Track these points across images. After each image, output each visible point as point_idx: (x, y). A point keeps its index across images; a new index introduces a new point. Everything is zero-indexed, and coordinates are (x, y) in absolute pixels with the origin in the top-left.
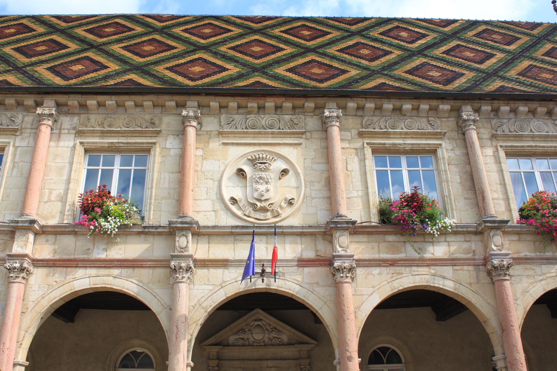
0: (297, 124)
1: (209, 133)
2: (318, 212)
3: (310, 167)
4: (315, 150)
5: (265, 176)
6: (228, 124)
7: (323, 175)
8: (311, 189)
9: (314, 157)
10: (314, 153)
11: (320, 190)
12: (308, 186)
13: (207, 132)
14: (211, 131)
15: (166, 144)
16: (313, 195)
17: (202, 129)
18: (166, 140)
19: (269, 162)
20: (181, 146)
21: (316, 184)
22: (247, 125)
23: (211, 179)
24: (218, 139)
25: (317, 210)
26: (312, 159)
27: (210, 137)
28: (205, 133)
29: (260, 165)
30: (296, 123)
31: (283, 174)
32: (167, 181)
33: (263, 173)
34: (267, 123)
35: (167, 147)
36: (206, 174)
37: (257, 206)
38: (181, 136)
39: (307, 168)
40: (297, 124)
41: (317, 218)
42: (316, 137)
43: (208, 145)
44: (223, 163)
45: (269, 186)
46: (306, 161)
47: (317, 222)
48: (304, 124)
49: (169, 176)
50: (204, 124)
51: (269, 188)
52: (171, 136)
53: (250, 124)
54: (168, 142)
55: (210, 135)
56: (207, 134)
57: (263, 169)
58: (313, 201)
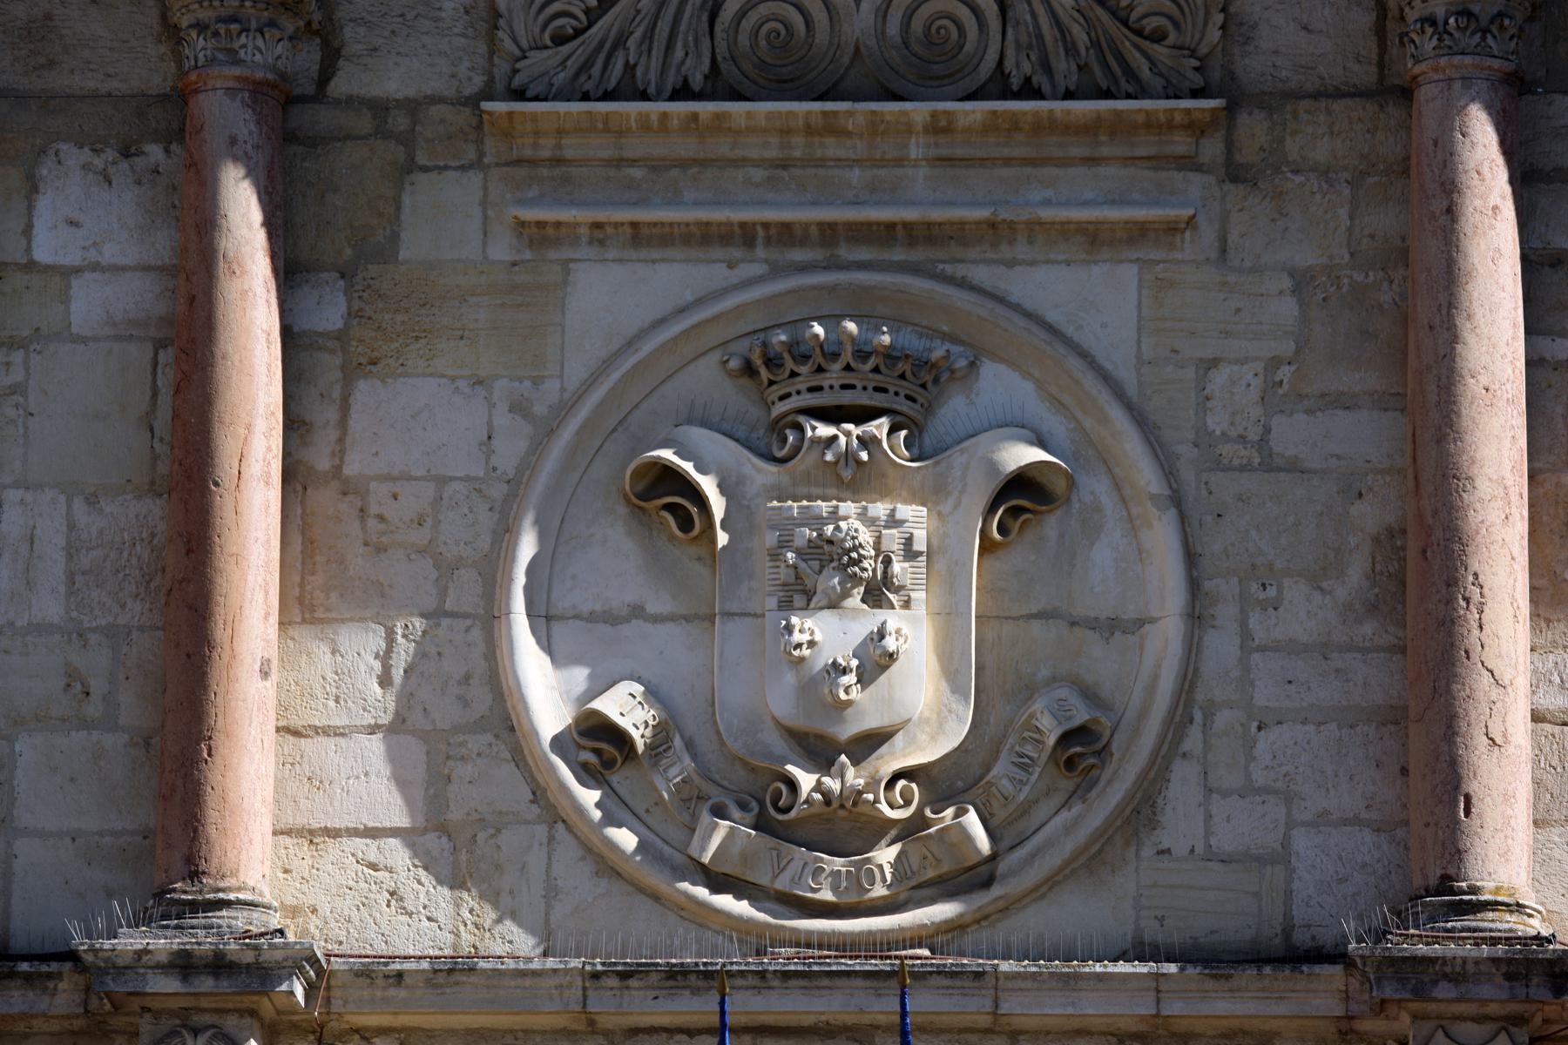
0: (1158, 37)
1: (400, 122)
2: (1302, 842)
3: (1254, 434)
4: (1302, 281)
5: (866, 536)
6: (560, 40)
7: (1358, 509)
8: (1246, 635)
9: (1287, 348)
10: (1288, 308)
11: (1324, 649)
12: (1226, 613)
13: (380, 108)
14: (413, 107)
15: (28, 231)
16: (1265, 695)
17: (340, 86)
18: (33, 187)
19: (904, 406)
20: (161, 245)
21: (1295, 592)
22: (722, 49)
23: (422, 551)
24: (475, 179)
25: (1290, 825)
26: (1274, 363)
27: (410, 167)
28: (365, 123)
29: (824, 430)
30: (1151, 24)
31: (1015, 512)
32: (53, 567)
33: (848, 508)
34: (893, 28)
35: (42, 254)
36: (374, 509)
37: (793, 785)
38: (155, 152)
39: (1226, 449)
40: (1158, 37)
41: (1288, 893)
42: (1321, 152)
43: (395, 238)
44: (519, 408)
45: (893, 619)
46: (1219, 378)
47: (1288, 931)
48: (1214, 35)
49: (72, 527)
50: (353, 37)
51: (891, 643)
52: (74, 156)
53: (744, 40)
54: (47, 208)
55: (407, 140)
56: (381, 132)
57: (847, 474)
58: (1264, 742)
